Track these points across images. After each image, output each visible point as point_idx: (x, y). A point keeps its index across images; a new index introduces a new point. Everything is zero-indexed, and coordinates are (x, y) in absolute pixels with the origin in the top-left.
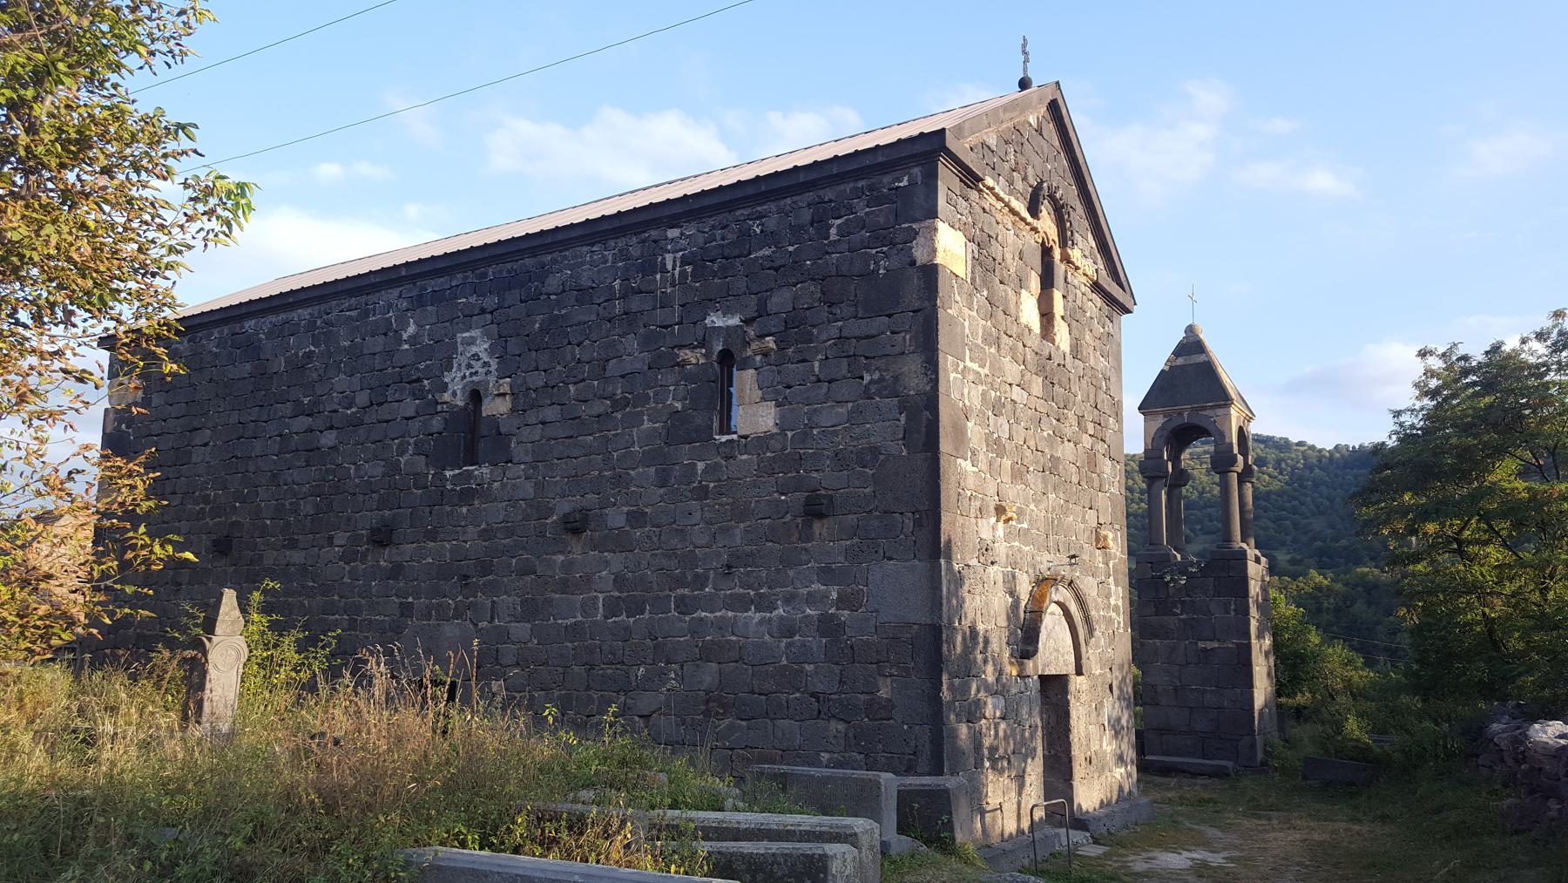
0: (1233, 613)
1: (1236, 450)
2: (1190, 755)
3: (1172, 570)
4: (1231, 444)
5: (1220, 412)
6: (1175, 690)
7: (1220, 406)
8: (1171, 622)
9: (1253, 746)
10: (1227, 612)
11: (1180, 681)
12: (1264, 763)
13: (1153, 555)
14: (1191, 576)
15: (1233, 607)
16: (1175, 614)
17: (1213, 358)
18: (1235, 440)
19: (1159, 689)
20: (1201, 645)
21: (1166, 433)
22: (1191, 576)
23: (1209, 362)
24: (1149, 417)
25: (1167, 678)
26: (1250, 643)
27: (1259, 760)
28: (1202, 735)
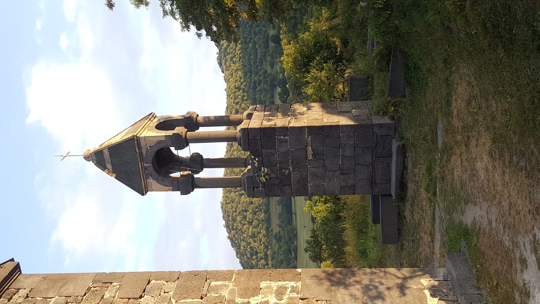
0: (287, 138)
1: (170, 133)
2: (389, 166)
3: (258, 176)
4: (165, 136)
5: (143, 144)
6: (343, 174)
7: (139, 144)
8: (295, 176)
9: (381, 126)
10: (286, 141)
11: (336, 171)
12: (392, 118)
13: (248, 187)
14: (262, 164)
15: (282, 137)
16: (290, 173)
17: (106, 144)
18: (163, 133)
19: (343, 184)
20: (310, 157)
21: (159, 178)
22: (262, 164)
23: (108, 148)
24: (149, 189)
25: (335, 179)
26: (308, 127)
27: (392, 122)
28: (374, 158)
